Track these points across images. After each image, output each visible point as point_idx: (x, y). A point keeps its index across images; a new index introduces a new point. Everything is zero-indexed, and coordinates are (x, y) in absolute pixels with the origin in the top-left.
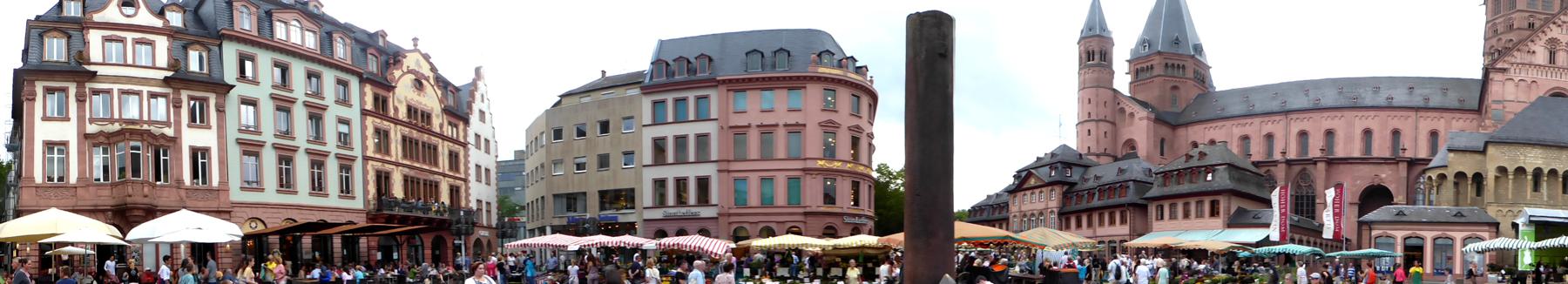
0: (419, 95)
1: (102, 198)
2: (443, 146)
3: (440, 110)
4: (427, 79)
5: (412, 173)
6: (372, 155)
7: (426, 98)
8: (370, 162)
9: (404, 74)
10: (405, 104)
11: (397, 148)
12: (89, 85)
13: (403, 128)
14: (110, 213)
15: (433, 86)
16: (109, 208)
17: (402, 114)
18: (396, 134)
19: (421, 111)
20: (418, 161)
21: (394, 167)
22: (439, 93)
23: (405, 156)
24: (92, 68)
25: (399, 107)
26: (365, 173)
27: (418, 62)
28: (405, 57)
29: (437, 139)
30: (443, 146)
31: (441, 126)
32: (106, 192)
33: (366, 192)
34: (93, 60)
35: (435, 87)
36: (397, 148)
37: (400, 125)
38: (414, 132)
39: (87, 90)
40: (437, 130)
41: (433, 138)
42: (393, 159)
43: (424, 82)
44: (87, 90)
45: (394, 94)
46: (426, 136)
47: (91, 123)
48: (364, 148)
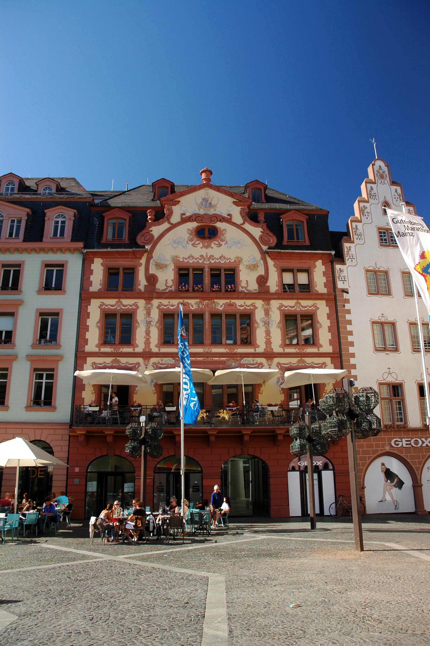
0: (207, 247)
2: (267, 312)
3: (258, 255)
4: (228, 220)
6: (97, 350)
9: (173, 226)
10: (172, 267)
11: (148, 333)
13: (165, 302)
18: (148, 313)
19: (212, 270)
21: (140, 360)
29: (249, 302)
30: (267, 312)
35: (248, 226)
36: (148, 333)
38: (192, 302)
41: (238, 302)
43: (218, 225)
46: (222, 302)
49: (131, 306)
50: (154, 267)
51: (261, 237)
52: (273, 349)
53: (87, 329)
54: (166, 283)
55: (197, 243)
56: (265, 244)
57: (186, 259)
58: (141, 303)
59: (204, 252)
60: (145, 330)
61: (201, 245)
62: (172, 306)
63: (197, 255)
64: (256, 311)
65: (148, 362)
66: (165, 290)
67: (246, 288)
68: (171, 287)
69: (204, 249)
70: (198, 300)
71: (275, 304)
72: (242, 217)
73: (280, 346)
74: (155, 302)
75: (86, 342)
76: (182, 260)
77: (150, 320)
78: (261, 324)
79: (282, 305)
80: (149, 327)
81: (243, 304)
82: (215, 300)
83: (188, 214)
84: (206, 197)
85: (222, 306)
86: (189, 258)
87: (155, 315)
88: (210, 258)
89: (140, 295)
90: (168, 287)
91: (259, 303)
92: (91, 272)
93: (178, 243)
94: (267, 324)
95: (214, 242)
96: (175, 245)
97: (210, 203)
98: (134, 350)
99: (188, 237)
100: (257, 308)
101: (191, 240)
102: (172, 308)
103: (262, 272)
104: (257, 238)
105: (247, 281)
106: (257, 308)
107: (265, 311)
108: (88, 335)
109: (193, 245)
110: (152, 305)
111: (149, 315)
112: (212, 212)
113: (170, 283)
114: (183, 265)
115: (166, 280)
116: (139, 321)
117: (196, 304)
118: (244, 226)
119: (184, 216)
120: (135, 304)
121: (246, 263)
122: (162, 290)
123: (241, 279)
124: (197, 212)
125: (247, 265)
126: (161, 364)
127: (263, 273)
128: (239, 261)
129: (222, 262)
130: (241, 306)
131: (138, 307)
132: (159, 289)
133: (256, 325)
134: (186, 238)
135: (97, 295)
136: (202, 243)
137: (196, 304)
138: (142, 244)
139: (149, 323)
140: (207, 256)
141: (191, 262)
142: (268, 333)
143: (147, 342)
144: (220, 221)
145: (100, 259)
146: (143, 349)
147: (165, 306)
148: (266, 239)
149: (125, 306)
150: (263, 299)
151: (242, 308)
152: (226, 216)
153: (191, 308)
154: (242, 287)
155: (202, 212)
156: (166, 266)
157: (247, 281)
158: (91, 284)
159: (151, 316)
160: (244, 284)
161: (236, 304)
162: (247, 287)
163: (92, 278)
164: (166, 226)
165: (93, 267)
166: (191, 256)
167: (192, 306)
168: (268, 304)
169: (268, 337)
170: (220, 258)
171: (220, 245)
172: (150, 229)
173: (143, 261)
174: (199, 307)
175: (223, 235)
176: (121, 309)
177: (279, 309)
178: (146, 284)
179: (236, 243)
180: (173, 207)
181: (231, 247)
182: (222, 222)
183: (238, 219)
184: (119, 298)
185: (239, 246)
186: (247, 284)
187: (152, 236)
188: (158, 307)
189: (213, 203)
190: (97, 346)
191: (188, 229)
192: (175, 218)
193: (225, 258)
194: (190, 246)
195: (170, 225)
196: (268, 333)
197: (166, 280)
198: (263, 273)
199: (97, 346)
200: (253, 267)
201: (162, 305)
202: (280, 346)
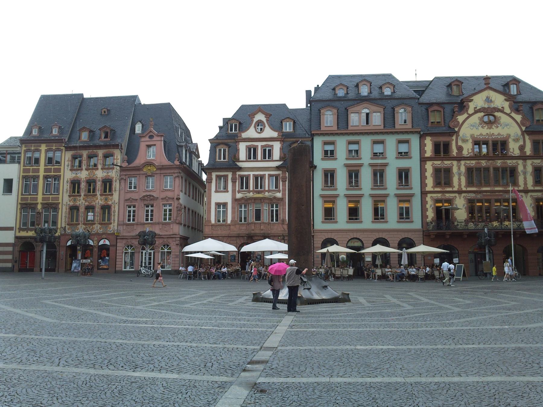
0: (490, 128)
1: (242, 230)
2: (525, 167)
3: (519, 133)
4: (502, 111)
5: (479, 196)
6: (432, 190)
7: (500, 128)
8: (429, 195)
9: (470, 116)
10: (471, 141)
11: (460, 179)
12: (238, 173)
13: (468, 162)
14: (246, 237)
15: (508, 115)
16: (245, 235)
17: (468, 148)
18: (459, 168)
19: (493, 141)
20: (487, 184)
21: (457, 195)
22: (518, 118)
23: (470, 183)
24: (240, 164)
25: (463, 145)
26: (423, 203)
27: (488, 100)
28: (472, 100)
29: (514, 161)
30: (525, 167)
31: (522, 148)
32: (244, 228)
33: (424, 216)
34: (241, 159)
35: (513, 115)
36: (460, 179)
37: (464, 160)
38: (483, 162)
39: (237, 176)
40: (517, 152)
41: (509, 161)
42: (455, 189)
43: (497, 114)
44: (237, 176)
45: (458, 136)
46: (499, 161)
47: (238, 193)
48: (423, 184)
49: (449, 164)
50: (460, 141)
51: (521, 121)
52: (528, 188)
53: (426, 178)
54: (468, 151)
55: (484, 126)
56: (524, 125)
57: (478, 136)
58: (455, 163)
59: (488, 131)
60: (458, 178)
61: (486, 127)
62: (472, 164)
63: (484, 133)
64: (519, 166)
65: (461, 195)
66: (468, 155)
67: (513, 153)
68: (471, 153)
69: (488, 129)
70: (486, 161)
71: (529, 162)
72: (510, 108)
73: (532, 186)
74: (463, 162)
75: (426, 185)
76: (476, 137)
77: (460, 172)
78: (521, 173)
79: (533, 163)
80: (460, 176)
81: (511, 162)
82: (496, 161)
83: (478, 108)
84: (488, 96)
85: (499, 164)
86: (480, 135)
87: (463, 169)
88: (492, 135)
89: (454, 159)
90: (469, 153)
91: (520, 162)
92: (425, 145)
93: (473, 126)
94: (525, 173)
95: (495, 125)
96: (472, 128)
97: (491, 100)
98: (453, 189)
99: (479, 122)
100: (519, 164)
101: (481, 124)
102: (472, 165)
103: (521, 143)
104: (519, 122)
105: (513, 148)
106: (519, 164)
107: (523, 166)
108: (427, 181)
109: (482, 127)
110: (461, 164)
111: (460, 169)
112: (492, 105)
113: (470, 151)
114: (477, 140)
115: (468, 149)
116: (454, 173)
117: (485, 162)
118: (511, 115)
119: (476, 109)
120: (452, 163)
121: (513, 138)
122: (466, 155)
123: (510, 147)
124: (484, 106)
125: (513, 139)
126: (468, 197)
127: (522, 143)
128: (509, 136)
129: (499, 137)
130: (510, 163)
131: (453, 165)
132: (464, 154)
133: (519, 174)
134: (478, 123)
135: (430, 159)
136: (487, 125)
137: (485, 162)
138: (453, 127)
139: (460, 175)
140: (490, 134)
141: (481, 137)
142: (525, 179)
143: (460, 185)
144: (498, 112)
145: (429, 137)
146: (458, 189)
147: (468, 164)
148: (524, 122)
149: (446, 164)
150: (523, 159)
151: (510, 165)
152: (500, 108)
153: (482, 165)
154: (511, 152)
155: (486, 106)
156: (467, 141)
157: (513, 148)
158: (425, 152)
159: (461, 170)
160: (511, 150)
161: (507, 163)
162: (513, 152)
163: (426, 149)
164: (465, 116)
165: (426, 142)
166: (481, 135)
167: (483, 164)
168: (525, 162)
169: (525, 181)
170: (499, 134)
171: (497, 127)
172: (457, 118)
173: (454, 138)
174: (487, 164)
175: (499, 120)
176: (444, 166)
177: (531, 164)
178: (457, 151)
179: (507, 125)
180: (470, 103)
181: (503, 128)
182: (498, 112)
183: (507, 110)
184: (442, 160)
185: (508, 127)
186: (513, 150)
187: (458, 122)
188: (464, 165)
189: (493, 99)
190: (432, 187)
191: (479, 117)
192: (471, 111)
193: (501, 135)
194: (480, 128)
195: (468, 115)
196: (525, 179)
197: (468, 149)
198: (522, 143)
199: (432, 187)
200: (516, 140)
201: (467, 163)
202: (532, 186)
